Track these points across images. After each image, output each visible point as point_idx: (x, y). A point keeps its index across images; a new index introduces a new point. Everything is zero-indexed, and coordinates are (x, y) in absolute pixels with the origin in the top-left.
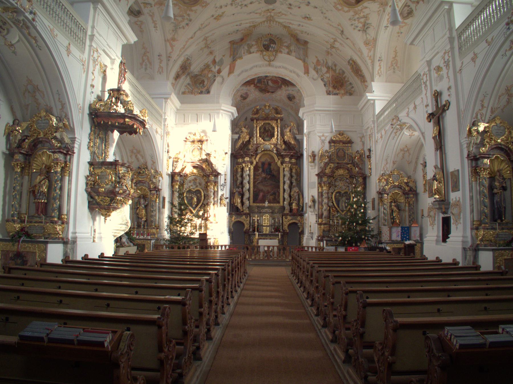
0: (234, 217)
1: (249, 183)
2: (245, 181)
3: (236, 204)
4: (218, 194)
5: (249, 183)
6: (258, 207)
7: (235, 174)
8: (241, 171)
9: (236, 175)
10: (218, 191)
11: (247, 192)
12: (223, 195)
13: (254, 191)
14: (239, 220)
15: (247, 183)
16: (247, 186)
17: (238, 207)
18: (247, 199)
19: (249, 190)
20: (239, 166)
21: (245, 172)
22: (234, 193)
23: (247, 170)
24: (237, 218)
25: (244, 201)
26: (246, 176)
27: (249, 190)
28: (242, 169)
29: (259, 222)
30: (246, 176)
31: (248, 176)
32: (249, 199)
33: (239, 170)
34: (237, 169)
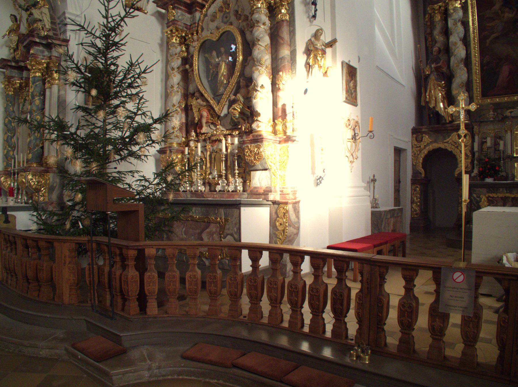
0: (426, 139)
1: (466, 41)
2: (455, 38)
3: (432, 106)
4: (292, 33)
5: (466, 41)
6: (497, 107)
7: (428, 31)
8: (441, 20)
9: (431, 34)
10: (292, 23)
11: (462, 66)
12: (317, 35)
13: (482, 65)
14: (442, 146)
15: (460, 44)
16: (460, 52)
17: (437, 112)
18: (461, 86)
19: (467, 61)
20: (436, 7)
21: (451, 15)
22: (427, 77)
23: (455, 9)
24: (435, 141)
25: (454, 92)
26: (455, 24)
27: (467, 61)
28: (446, 14)
29: (501, 147)
30: (455, 24)
31: (459, 24)
32: (468, 87)
33: (438, 18)
34: (431, 18)
